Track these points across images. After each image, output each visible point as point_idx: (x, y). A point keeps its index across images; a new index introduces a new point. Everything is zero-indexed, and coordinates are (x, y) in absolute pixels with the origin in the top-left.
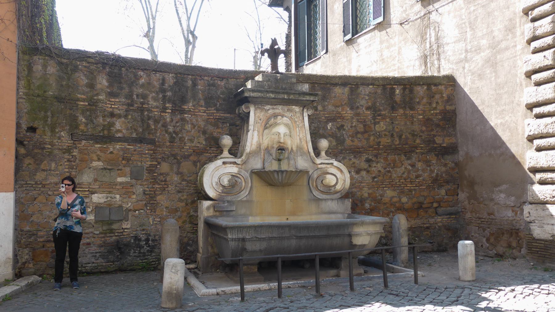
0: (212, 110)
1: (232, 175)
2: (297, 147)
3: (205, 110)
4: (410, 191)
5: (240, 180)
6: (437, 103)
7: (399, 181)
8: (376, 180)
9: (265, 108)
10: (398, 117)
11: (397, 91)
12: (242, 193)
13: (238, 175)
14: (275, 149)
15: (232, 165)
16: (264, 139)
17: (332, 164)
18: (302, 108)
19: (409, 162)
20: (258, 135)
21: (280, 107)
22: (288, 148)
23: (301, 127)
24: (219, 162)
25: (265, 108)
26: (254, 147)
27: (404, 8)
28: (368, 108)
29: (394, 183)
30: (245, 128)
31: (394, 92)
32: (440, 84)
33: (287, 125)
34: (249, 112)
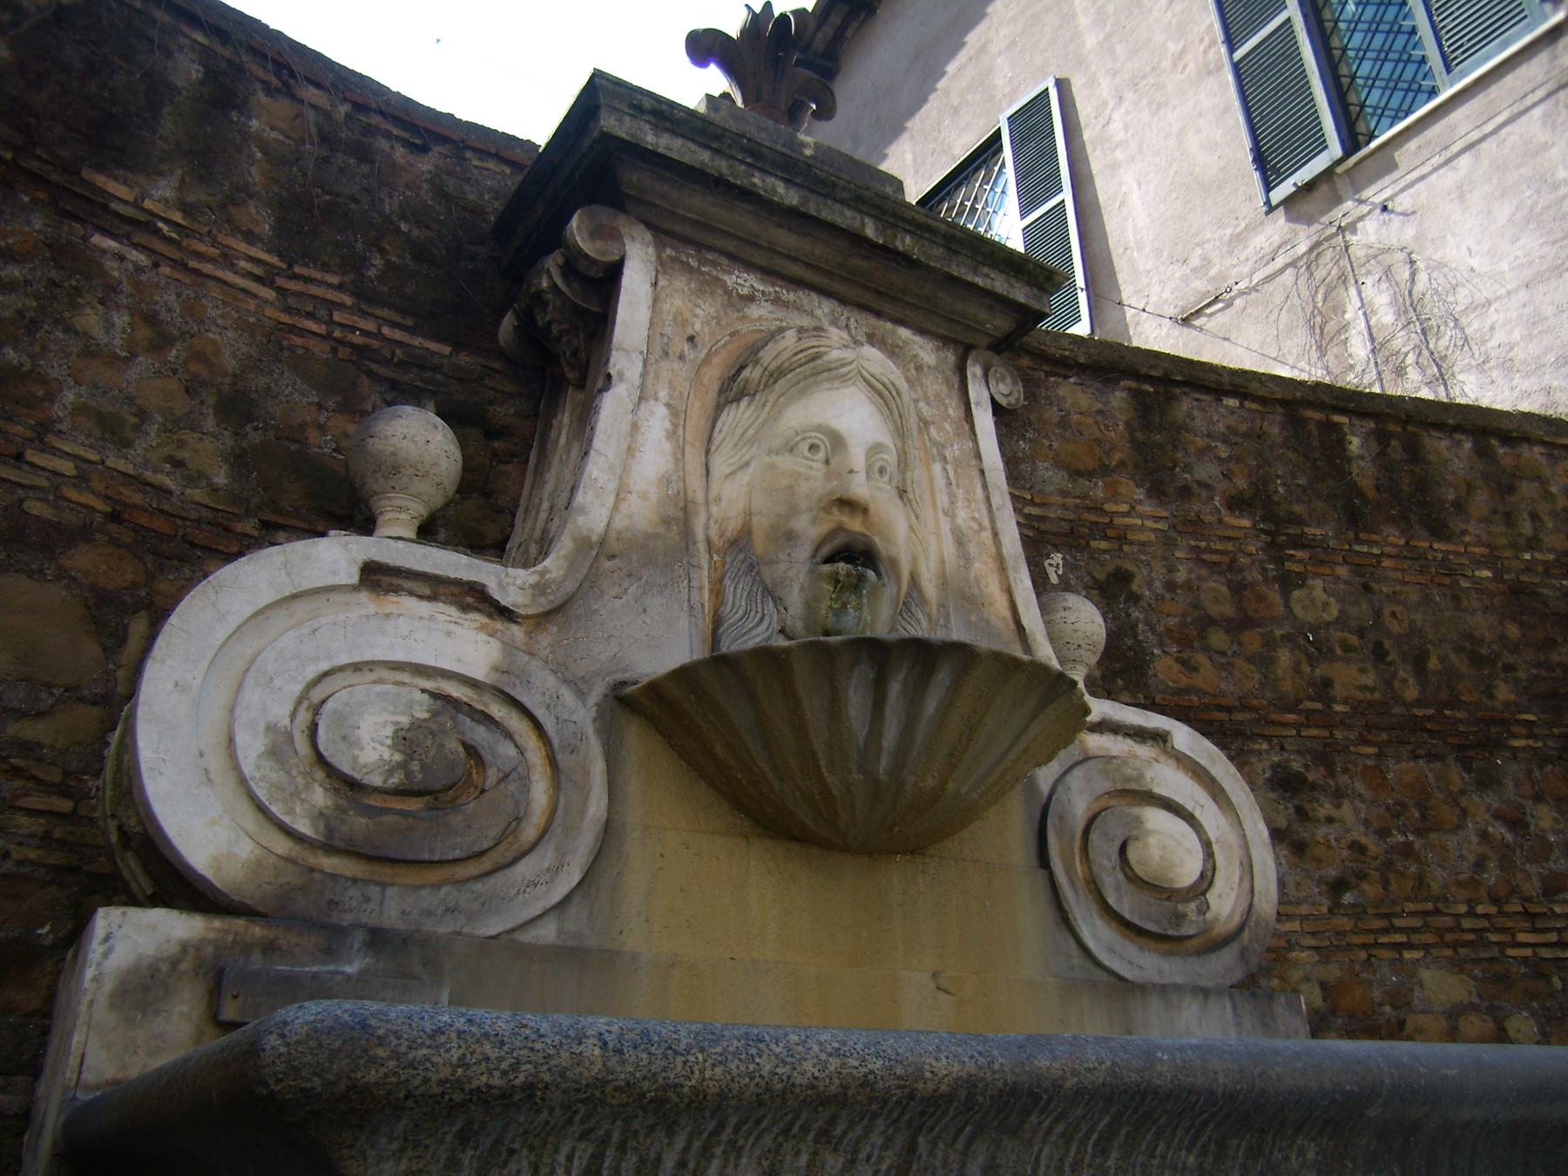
0: (326, 284)
2: (943, 582)
4: (1539, 970)
5: (512, 751)
6: (1534, 516)
7: (1471, 913)
8: (1348, 898)
10: (1386, 563)
11: (1355, 444)
12: (524, 869)
13: (497, 710)
14: (803, 553)
15: (445, 612)
16: (720, 465)
18: (951, 358)
19: (1492, 799)
20: (672, 435)
22: (894, 563)
23: (958, 464)
25: (730, 280)
26: (641, 510)
27: (1195, 261)
28: (1236, 503)
29: (1448, 922)
30: (565, 418)
31: (1342, 443)
32: (1526, 439)
33: (883, 395)
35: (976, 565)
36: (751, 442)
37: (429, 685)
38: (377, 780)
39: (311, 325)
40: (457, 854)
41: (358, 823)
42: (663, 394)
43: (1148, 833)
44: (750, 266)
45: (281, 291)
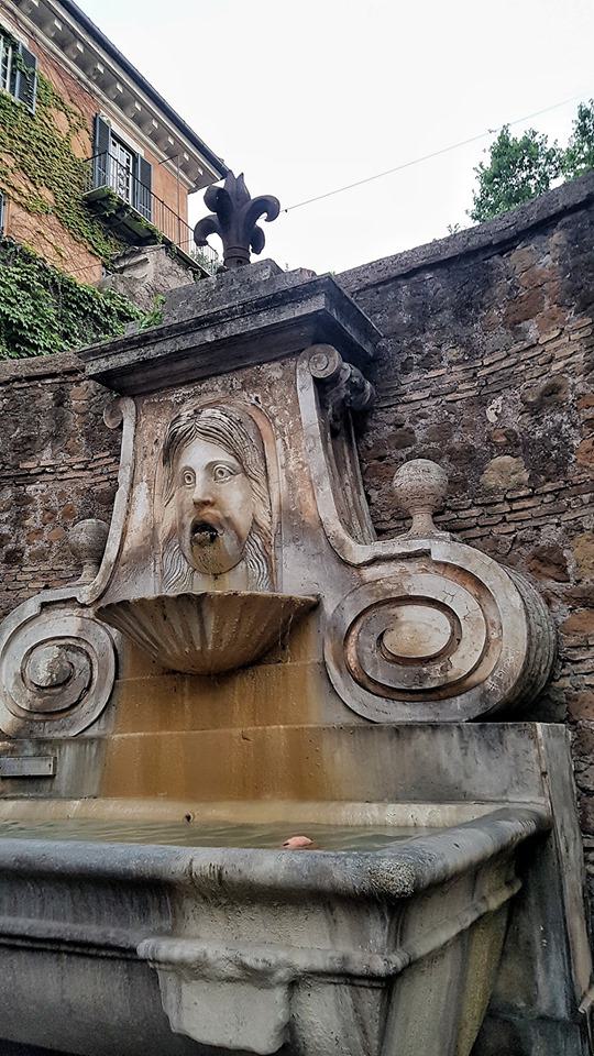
1: (60, 646)
3: (89, 462)
5: (84, 660)
9: (172, 398)
13: (84, 646)
15: (68, 611)
17: (426, 553)
21: (217, 384)
22: (228, 520)
23: (292, 432)
24: (31, 607)
25: (172, 398)
26: (133, 540)
34: (121, 427)
35: (300, 490)
36: (169, 486)
37: (62, 642)
38: (43, 684)
39: (101, 478)
40: (67, 706)
41: (38, 701)
42: (145, 477)
43: (401, 624)
44: (183, 384)
45: (91, 470)
